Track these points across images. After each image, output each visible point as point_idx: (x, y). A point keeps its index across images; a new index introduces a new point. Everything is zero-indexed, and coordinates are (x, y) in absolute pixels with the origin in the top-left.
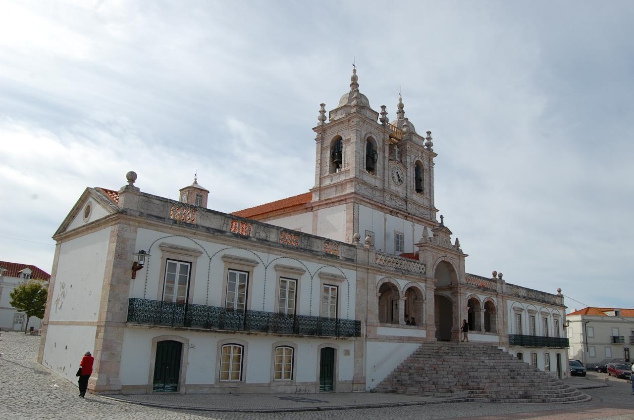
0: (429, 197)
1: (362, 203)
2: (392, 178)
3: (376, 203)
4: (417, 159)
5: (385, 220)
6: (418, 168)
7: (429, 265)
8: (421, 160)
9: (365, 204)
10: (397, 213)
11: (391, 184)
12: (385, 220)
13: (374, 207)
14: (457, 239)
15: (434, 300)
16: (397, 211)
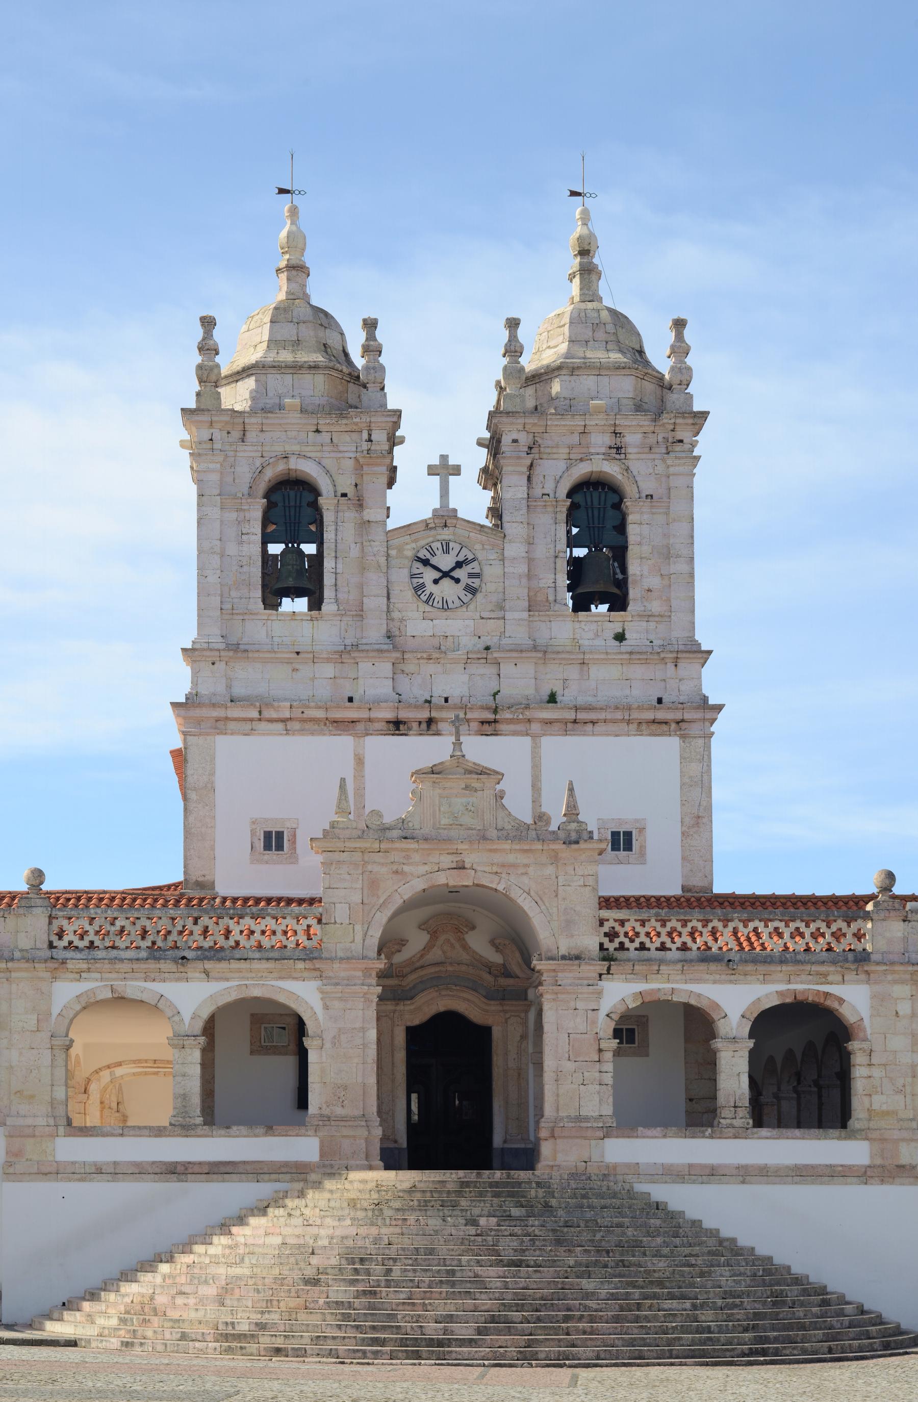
0: (656, 606)
1: (232, 725)
2: (409, 593)
3: (297, 713)
4: (581, 471)
5: (359, 761)
6: (597, 510)
7: (341, 913)
8: (611, 469)
9: (247, 726)
10: (430, 722)
11: (402, 620)
12: (359, 761)
13: (296, 725)
14: (571, 783)
15: (372, 1034)
16: (425, 715)
